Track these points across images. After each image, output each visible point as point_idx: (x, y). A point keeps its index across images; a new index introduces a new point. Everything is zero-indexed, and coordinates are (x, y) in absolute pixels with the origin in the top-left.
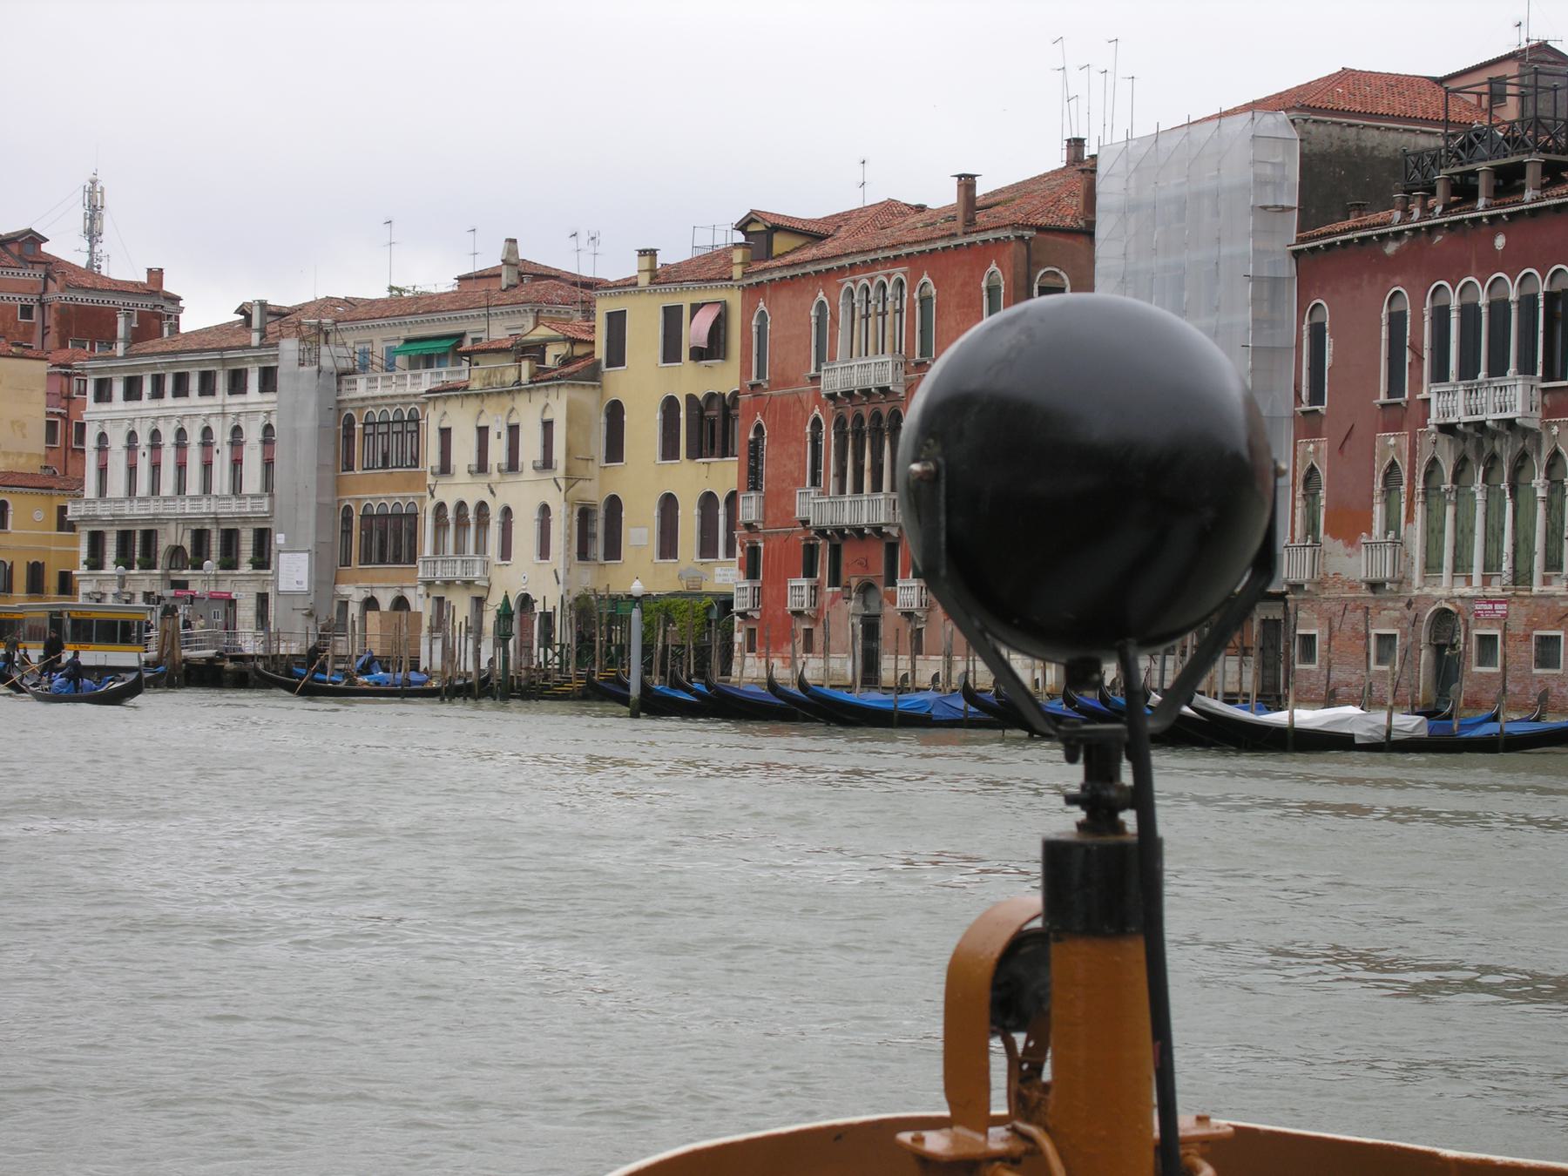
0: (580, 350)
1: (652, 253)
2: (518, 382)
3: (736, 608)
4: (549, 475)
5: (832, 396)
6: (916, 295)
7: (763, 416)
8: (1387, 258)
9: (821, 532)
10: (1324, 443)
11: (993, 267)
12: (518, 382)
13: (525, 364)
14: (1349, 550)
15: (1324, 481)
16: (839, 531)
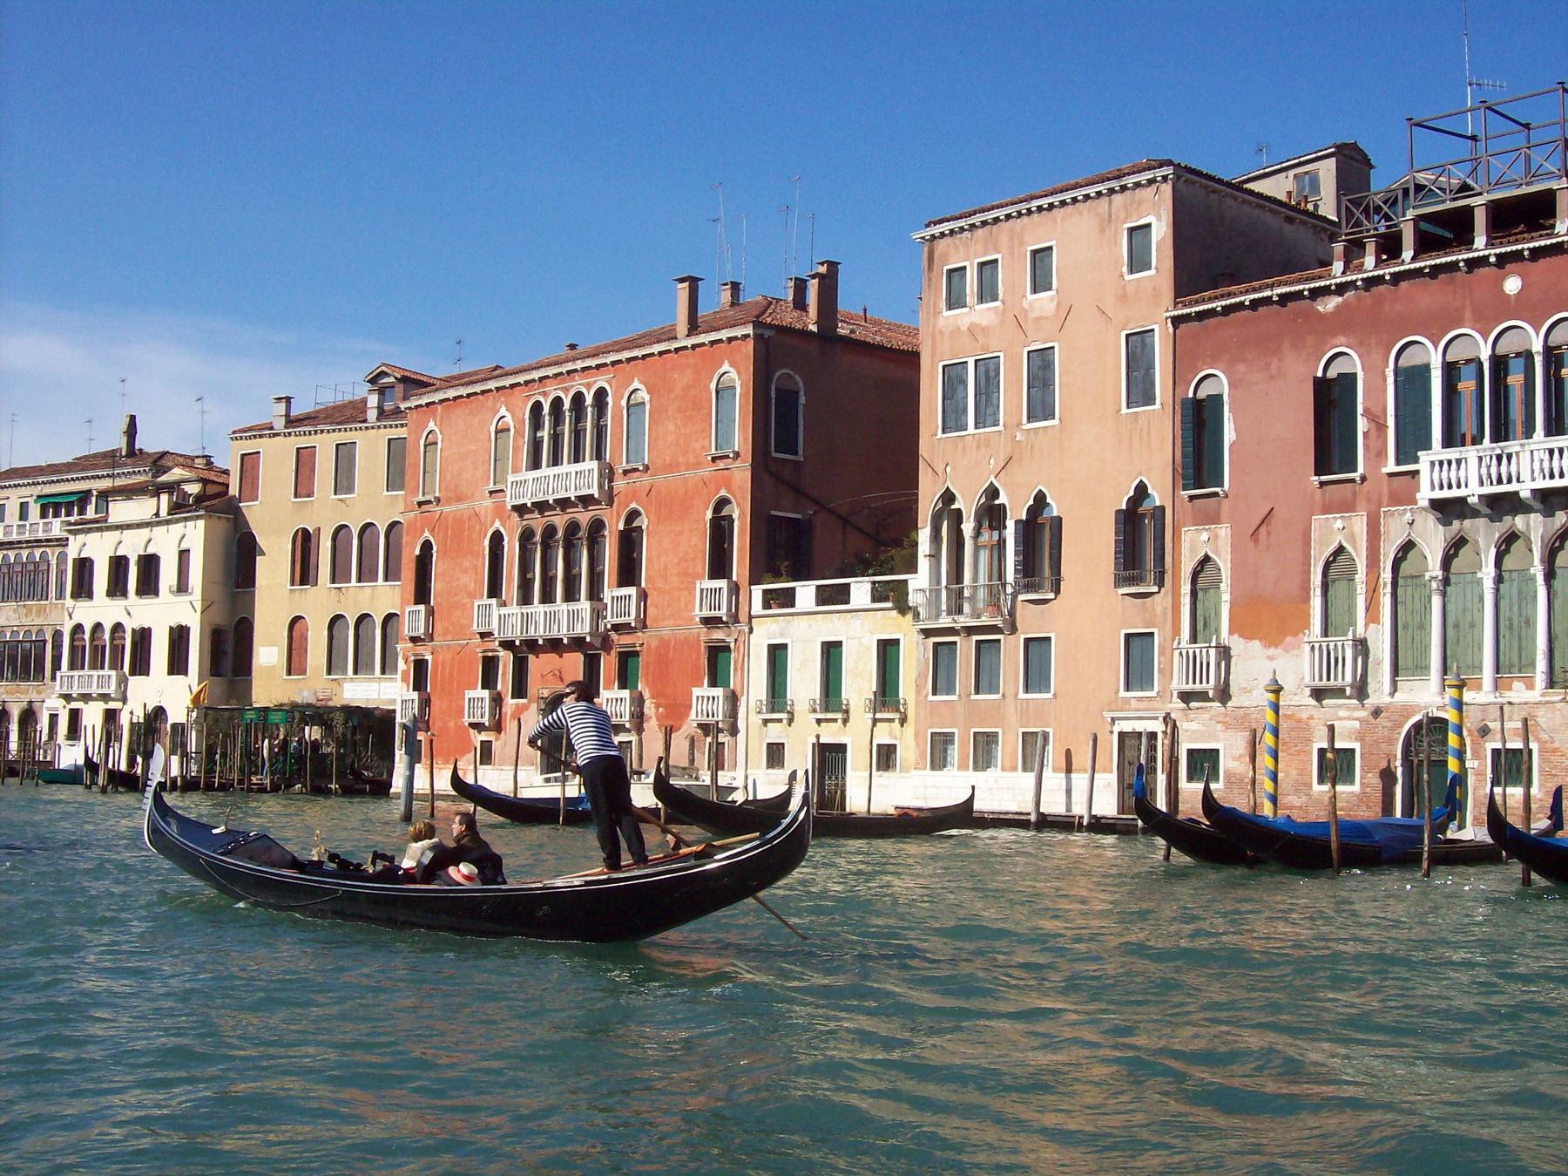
0: (211, 490)
1: (288, 400)
2: (157, 514)
3: (398, 719)
4: (184, 598)
5: (521, 510)
6: (624, 403)
7: (432, 532)
8: (1323, 316)
9: (507, 645)
10: (1224, 531)
11: (726, 367)
12: (157, 514)
13: (164, 498)
14: (1272, 651)
15: (1226, 574)
16: (531, 645)
